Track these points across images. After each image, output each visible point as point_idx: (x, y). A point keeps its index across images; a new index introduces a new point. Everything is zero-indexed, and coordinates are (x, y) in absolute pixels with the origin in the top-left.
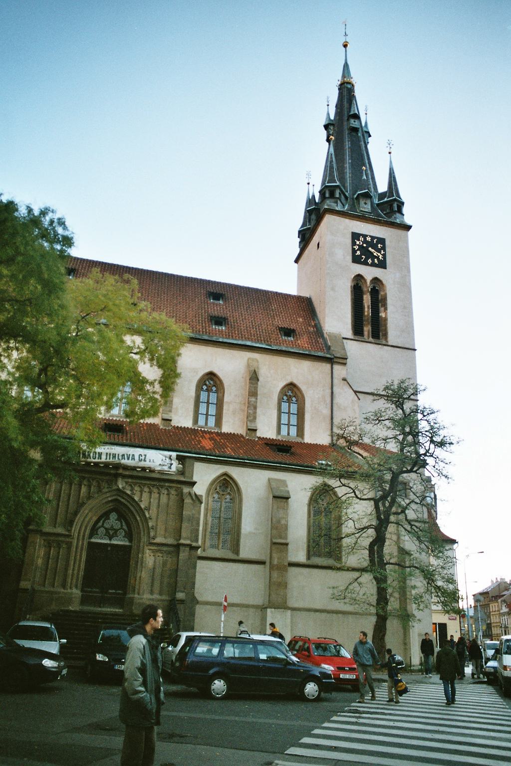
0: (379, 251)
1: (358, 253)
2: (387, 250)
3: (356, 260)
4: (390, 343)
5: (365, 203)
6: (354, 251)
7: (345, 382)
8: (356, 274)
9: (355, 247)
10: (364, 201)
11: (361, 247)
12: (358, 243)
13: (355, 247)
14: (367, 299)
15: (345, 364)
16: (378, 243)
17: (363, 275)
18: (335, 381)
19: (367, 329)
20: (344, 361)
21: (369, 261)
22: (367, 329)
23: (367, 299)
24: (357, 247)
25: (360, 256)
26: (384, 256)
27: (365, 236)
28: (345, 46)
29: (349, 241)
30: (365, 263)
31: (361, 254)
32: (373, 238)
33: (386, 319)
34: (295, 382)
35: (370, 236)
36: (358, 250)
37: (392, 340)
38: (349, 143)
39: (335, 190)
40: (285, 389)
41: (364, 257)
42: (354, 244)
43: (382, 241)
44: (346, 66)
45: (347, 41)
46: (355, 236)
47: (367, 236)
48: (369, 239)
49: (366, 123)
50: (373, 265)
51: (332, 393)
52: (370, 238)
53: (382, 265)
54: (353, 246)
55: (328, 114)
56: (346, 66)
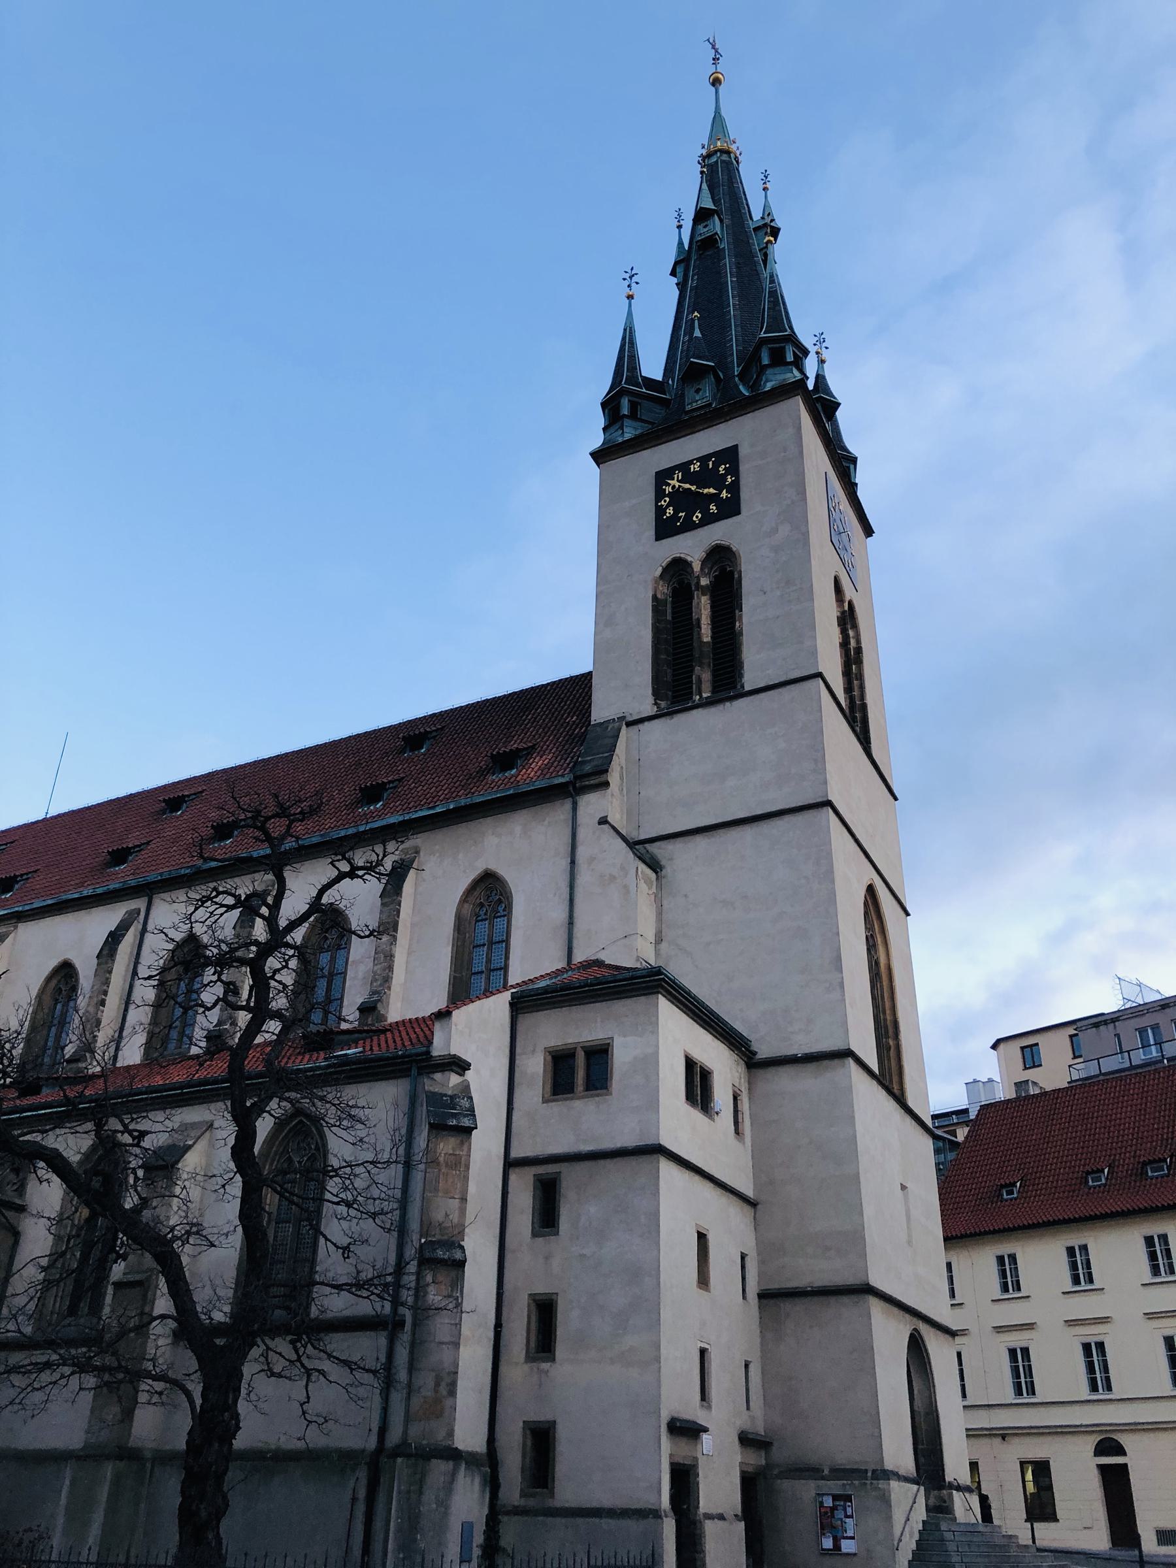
0: (719, 483)
1: (670, 511)
2: (743, 468)
3: (665, 529)
4: (747, 688)
5: (698, 391)
6: (660, 511)
7: (606, 827)
8: (664, 564)
9: (663, 503)
10: (693, 390)
11: (676, 494)
12: (668, 489)
13: (663, 503)
14: (703, 607)
15: (606, 784)
16: (716, 465)
17: (682, 556)
18: (582, 834)
19: (704, 676)
20: (602, 779)
21: (694, 519)
22: (704, 676)
23: (703, 607)
24: (667, 499)
25: (675, 517)
26: (735, 488)
27: (684, 467)
28: (716, 82)
29: (651, 495)
30: (689, 526)
31: (676, 512)
32: (703, 460)
33: (741, 633)
34: (493, 866)
35: (698, 459)
36: (668, 506)
37: (751, 679)
38: (696, 277)
39: (620, 402)
40: (476, 893)
41: (684, 514)
42: (659, 494)
43: (730, 455)
44: (718, 121)
45: (718, 70)
46: (662, 477)
47: (691, 462)
48: (695, 467)
49: (766, 206)
50: (708, 520)
51: (573, 862)
52: (698, 464)
53: (731, 508)
54: (658, 499)
55: (681, 243)
56: (718, 121)
